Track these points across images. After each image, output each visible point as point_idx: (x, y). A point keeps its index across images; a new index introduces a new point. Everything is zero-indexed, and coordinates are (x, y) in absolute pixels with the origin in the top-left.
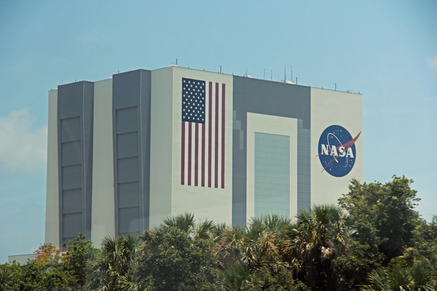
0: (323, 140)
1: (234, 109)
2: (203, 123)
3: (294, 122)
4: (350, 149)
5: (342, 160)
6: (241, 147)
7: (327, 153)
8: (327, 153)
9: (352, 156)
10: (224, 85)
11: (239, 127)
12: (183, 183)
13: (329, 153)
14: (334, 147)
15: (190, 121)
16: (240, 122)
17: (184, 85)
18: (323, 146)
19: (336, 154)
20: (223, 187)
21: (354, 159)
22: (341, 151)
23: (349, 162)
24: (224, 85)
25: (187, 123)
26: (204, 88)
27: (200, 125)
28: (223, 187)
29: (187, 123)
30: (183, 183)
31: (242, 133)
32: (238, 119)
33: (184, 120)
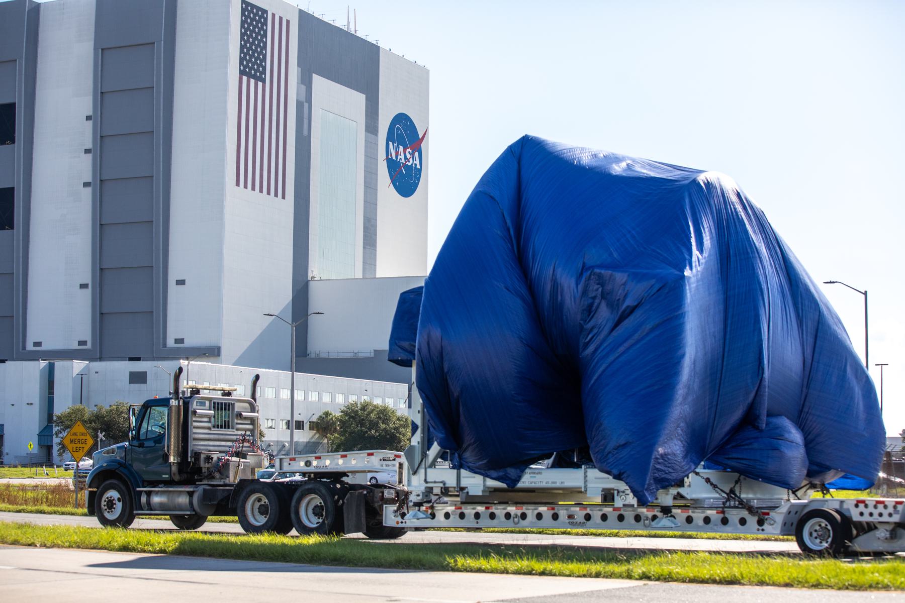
1: (299, 65)
2: (264, 81)
4: (416, 154)
6: (305, 133)
7: (394, 158)
8: (394, 158)
9: (418, 167)
10: (288, 22)
11: (303, 98)
12: (238, 184)
13: (397, 157)
14: (401, 148)
15: (249, 76)
16: (304, 87)
17: (243, 11)
18: (391, 143)
19: (403, 161)
20: (284, 197)
21: (420, 170)
22: (408, 156)
23: (416, 175)
24: (288, 22)
25: (245, 78)
26: (266, 20)
27: (260, 84)
28: (284, 197)
29: (245, 78)
30: (238, 184)
31: (306, 105)
32: (302, 83)
33: (242, 73)
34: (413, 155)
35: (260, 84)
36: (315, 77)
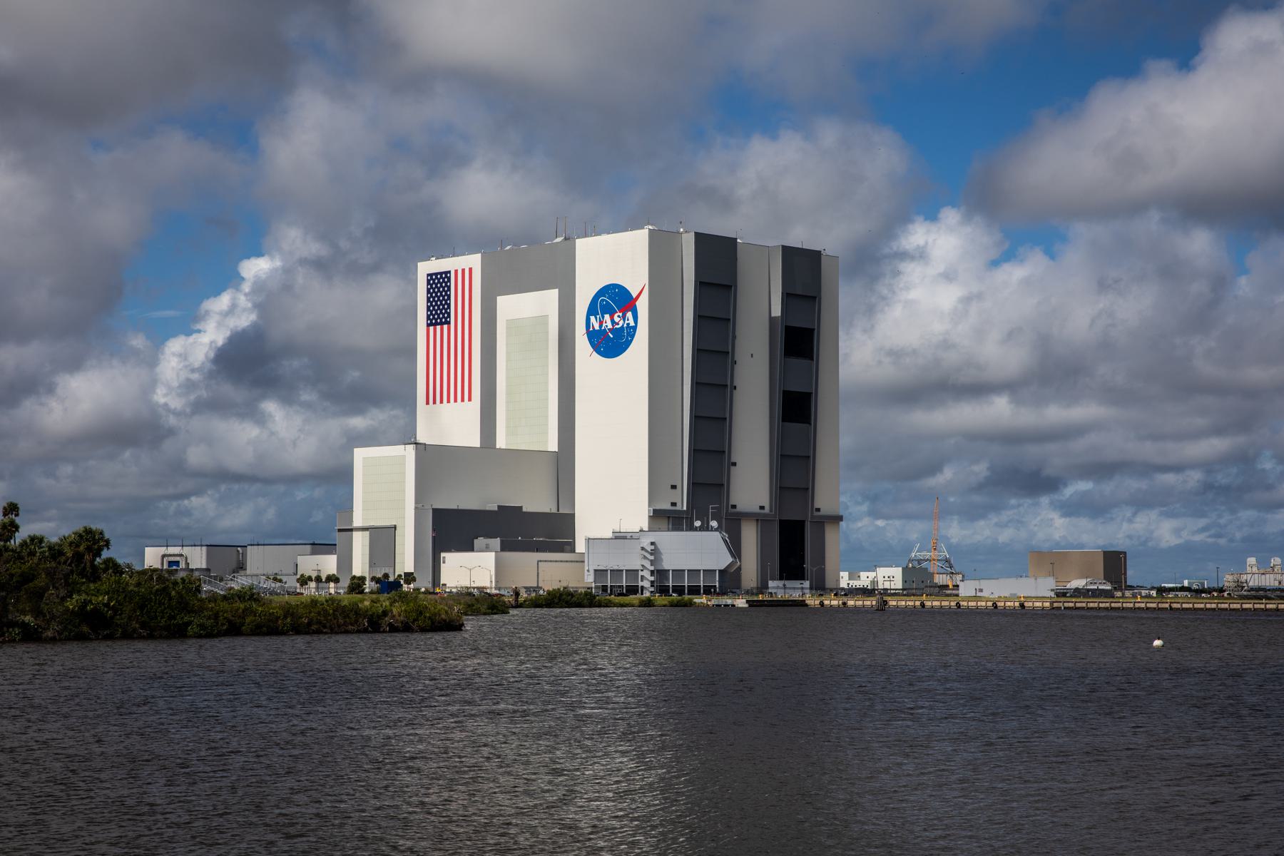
0: (592, 311)
2: (449, 323)
3: (553, 294)
4: (629, 315)
5: (618, 332)
7: (597, 328)
8: (597, 328)
9: (632, 324)
10: (470, 270)
14: (607, 317)
18: (592, 318)
19: (610, 326)
20: (470, 399)
21: (635, 328)
24: (470, 270)
26: (449, 279)
28: (470, 399)
34: (624, 317)
35: (445, 327)
36: (499, 299)
